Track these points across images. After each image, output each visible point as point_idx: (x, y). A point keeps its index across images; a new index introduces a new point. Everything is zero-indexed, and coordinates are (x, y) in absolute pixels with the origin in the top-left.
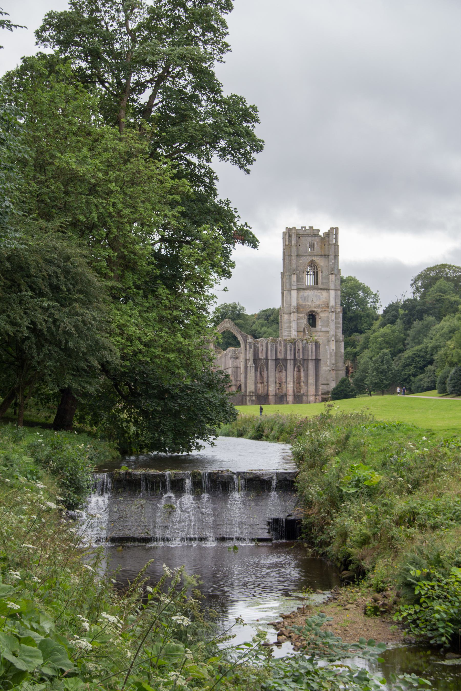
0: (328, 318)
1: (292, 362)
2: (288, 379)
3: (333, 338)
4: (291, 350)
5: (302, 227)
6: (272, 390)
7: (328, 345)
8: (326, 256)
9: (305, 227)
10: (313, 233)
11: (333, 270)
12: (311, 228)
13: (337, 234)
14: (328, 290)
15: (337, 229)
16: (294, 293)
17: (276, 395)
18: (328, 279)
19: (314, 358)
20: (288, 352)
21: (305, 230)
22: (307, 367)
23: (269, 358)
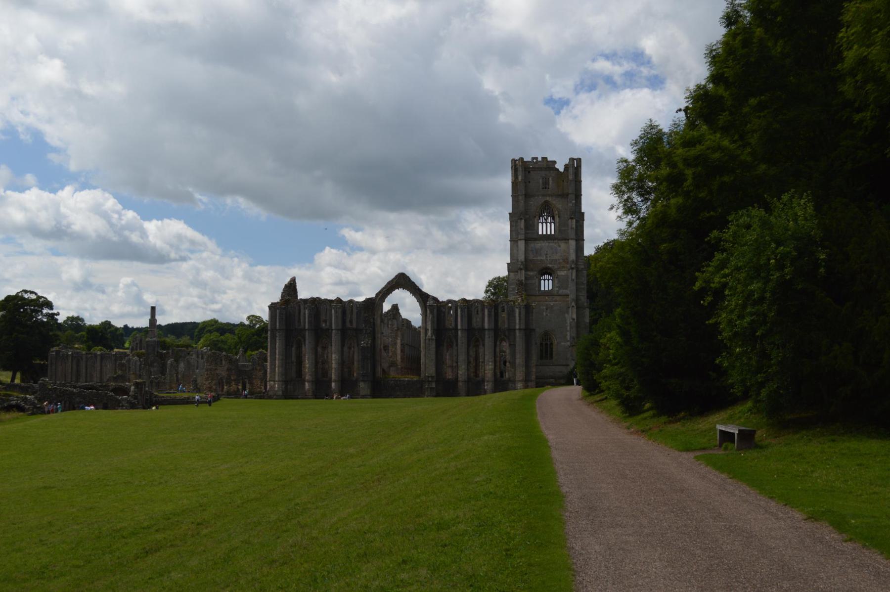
1: (492, 333)
2: (487, 358)
3: (573, 304)
4: (489, 315)
5: (533, 159)
6: (462, 373)
7: (568, 313)
8: (564, 196)
9: (537, 158)
10: (548, 165)
12: (544, 159)
14: (566, 240)
15: (579, 160)
16: (522, 244)
17: (468, 381)
21: (537, 162)
23: (459, 327)
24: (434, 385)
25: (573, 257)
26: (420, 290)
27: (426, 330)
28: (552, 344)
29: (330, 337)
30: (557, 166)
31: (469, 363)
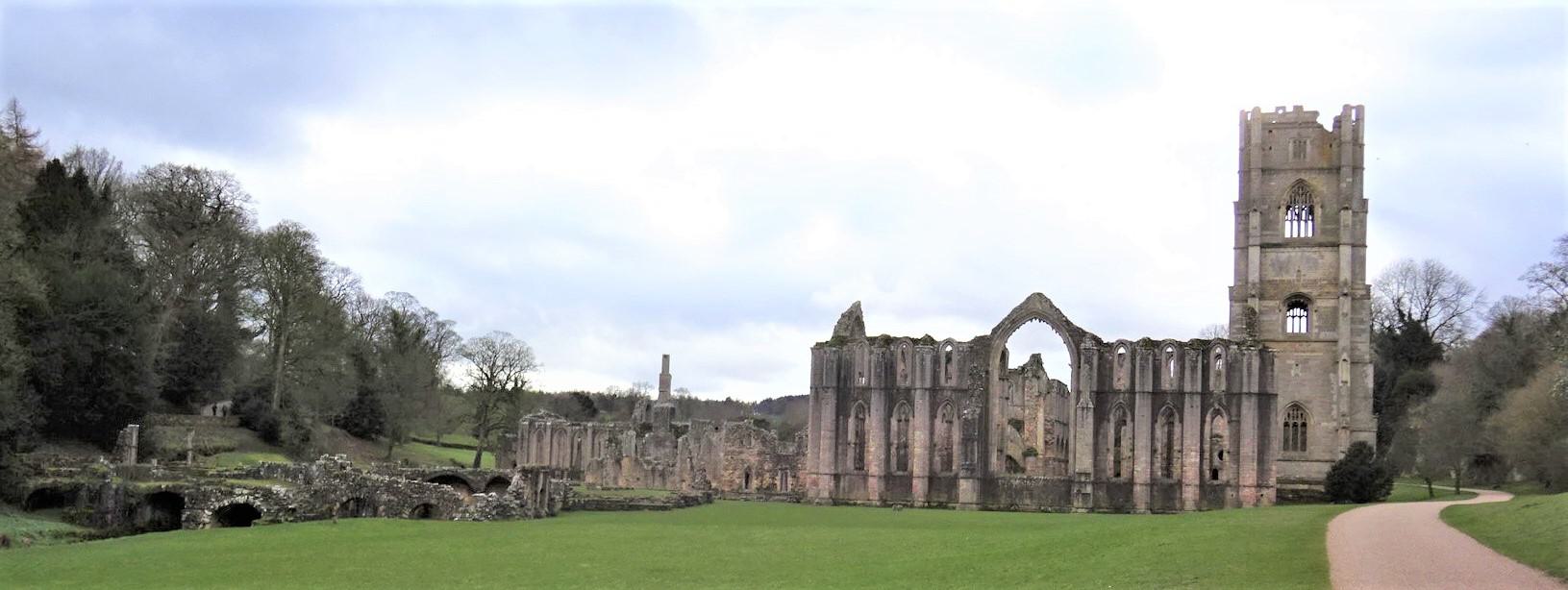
0: (1336, 309)
1: (1197, 400)
2: (1187, 442)
3: (1345, 356)
4: (1194, 369)
6: (1141, 470)
7: (1335, 372)
10: (1303, 121)
11: (1349, 199)
12: (1298, 109)
13: (1360, 119)
15: (1360, 109)
16: (1254, 253)
17: (1153, 483)
18: (1338, 221)
19: (1255, 389)
20: (1187, 373)
21: (1285, 114)
22: (1239, 415)
24: (1089, 489)
25: (1345, 274)
26: (1068, 322)
27: (1079, 393)
28: (1304, 425)
29: (911, 402)
30: (1319, 120)
31: (1154, 451)
